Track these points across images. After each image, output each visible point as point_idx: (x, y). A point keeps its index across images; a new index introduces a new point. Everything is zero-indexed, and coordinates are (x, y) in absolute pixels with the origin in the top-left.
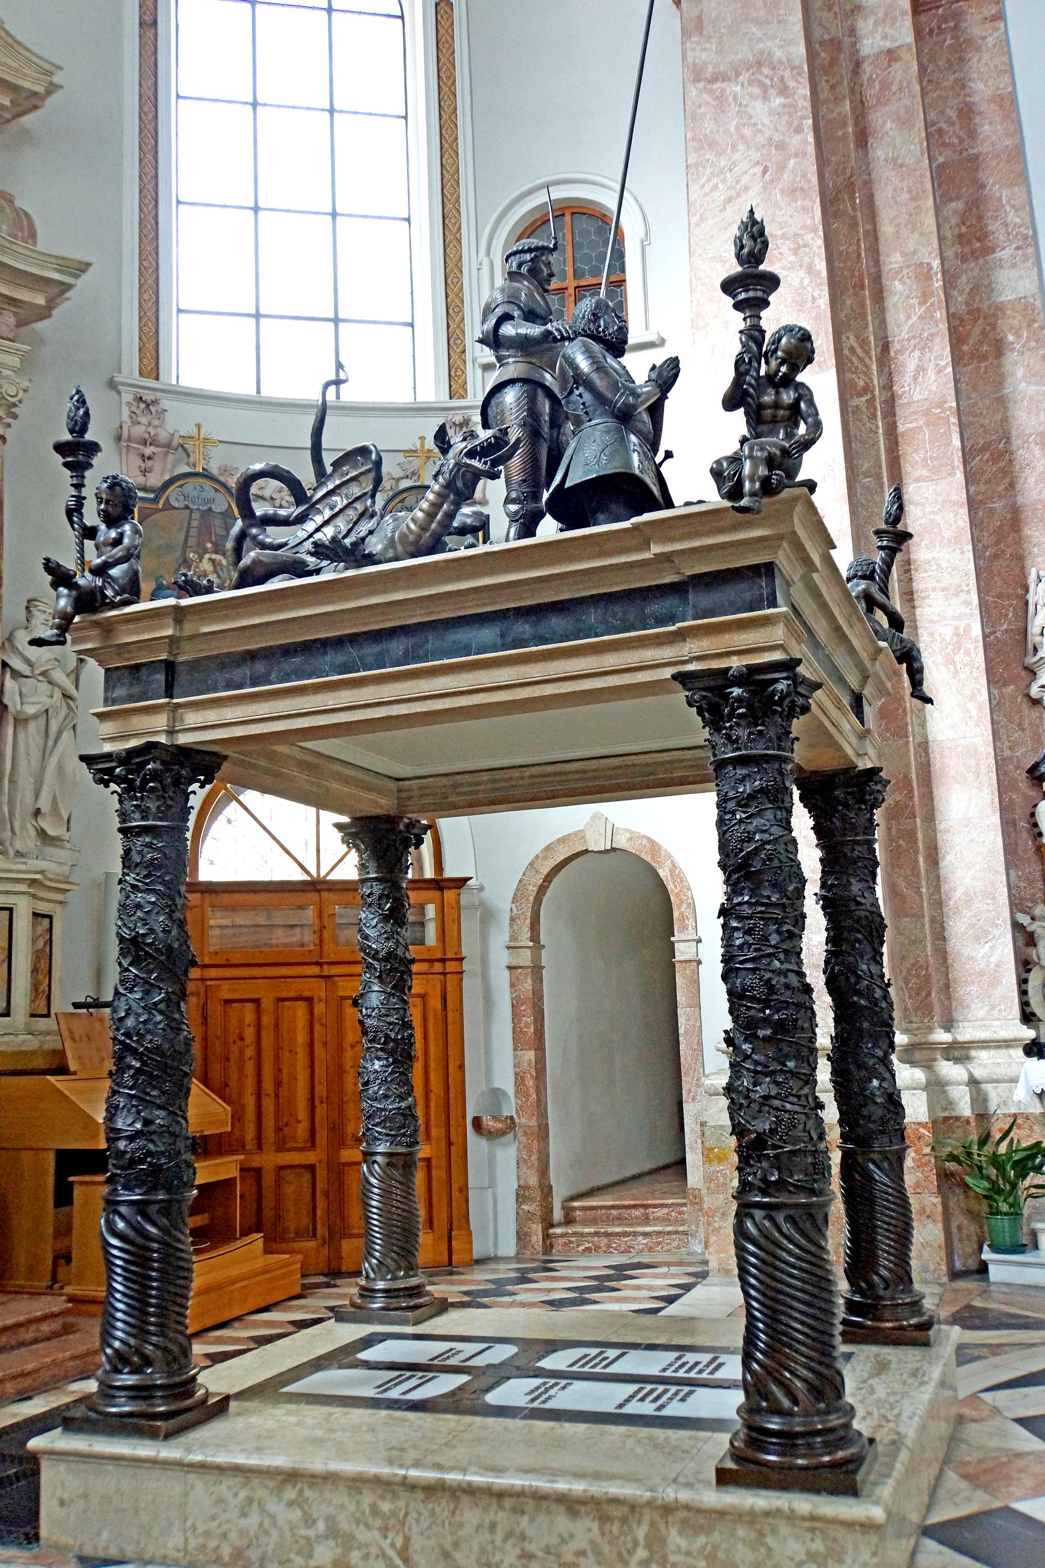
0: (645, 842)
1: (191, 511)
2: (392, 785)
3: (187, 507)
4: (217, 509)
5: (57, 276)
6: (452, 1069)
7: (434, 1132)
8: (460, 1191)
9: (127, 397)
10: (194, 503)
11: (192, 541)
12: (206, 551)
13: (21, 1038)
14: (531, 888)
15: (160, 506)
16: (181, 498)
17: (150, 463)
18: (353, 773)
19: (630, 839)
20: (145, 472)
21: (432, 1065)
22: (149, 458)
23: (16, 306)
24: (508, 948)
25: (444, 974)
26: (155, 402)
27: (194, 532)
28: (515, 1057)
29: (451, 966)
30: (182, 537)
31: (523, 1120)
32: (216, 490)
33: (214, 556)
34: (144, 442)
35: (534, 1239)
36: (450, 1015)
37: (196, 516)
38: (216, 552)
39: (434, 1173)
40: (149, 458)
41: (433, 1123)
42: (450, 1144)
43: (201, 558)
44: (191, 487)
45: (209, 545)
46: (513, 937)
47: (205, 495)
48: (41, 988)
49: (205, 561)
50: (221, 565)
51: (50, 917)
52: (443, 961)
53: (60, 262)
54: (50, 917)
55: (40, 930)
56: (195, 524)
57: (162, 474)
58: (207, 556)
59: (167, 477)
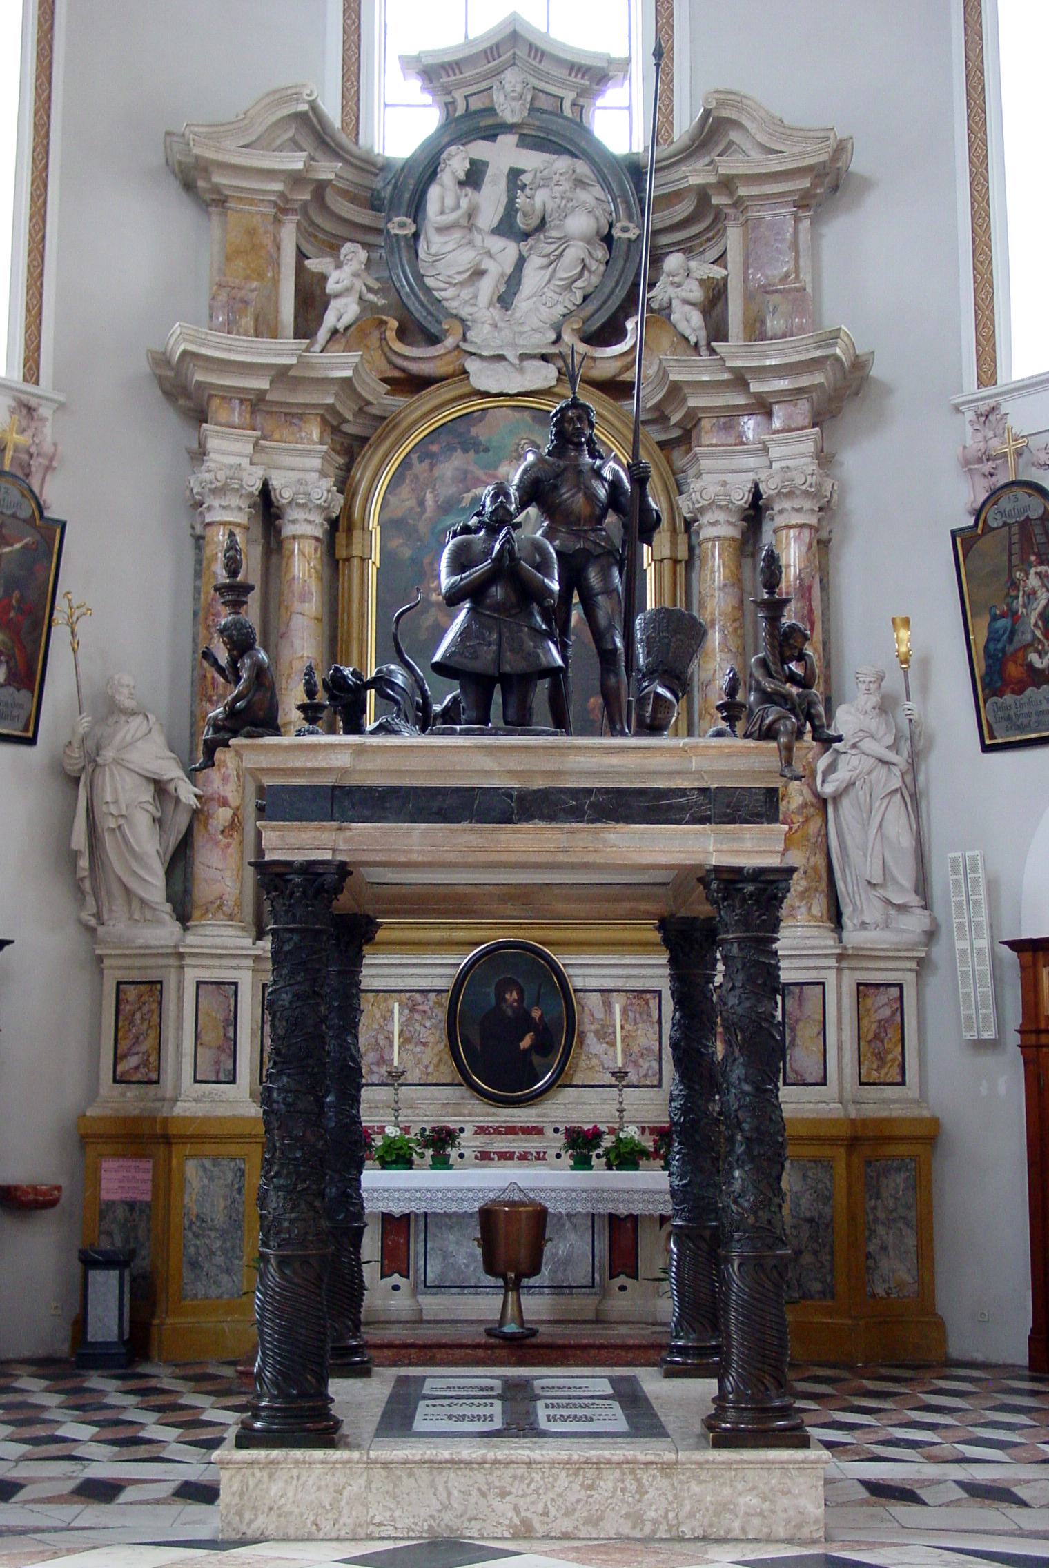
3: (1005, 524)
5: (818, 353)
9: (970, 415)
10: (1010, 516)
12: (1031, 565)
15: (979, 531)
16: (998, 517)
23: (806, 392)
26: (993, 409)
27: (1016, 548)
30: (1005, 558)
32: (1030, 495)
34: (980, 460)
37: (1015, 530)
38: (1041, 563)
43: (1027, 575)
44: (1005, 503)
45: (1033, 558)
47: (1020, 505)
49: (1032, 576)
56: (1015, 539)
58: (1033, 571)
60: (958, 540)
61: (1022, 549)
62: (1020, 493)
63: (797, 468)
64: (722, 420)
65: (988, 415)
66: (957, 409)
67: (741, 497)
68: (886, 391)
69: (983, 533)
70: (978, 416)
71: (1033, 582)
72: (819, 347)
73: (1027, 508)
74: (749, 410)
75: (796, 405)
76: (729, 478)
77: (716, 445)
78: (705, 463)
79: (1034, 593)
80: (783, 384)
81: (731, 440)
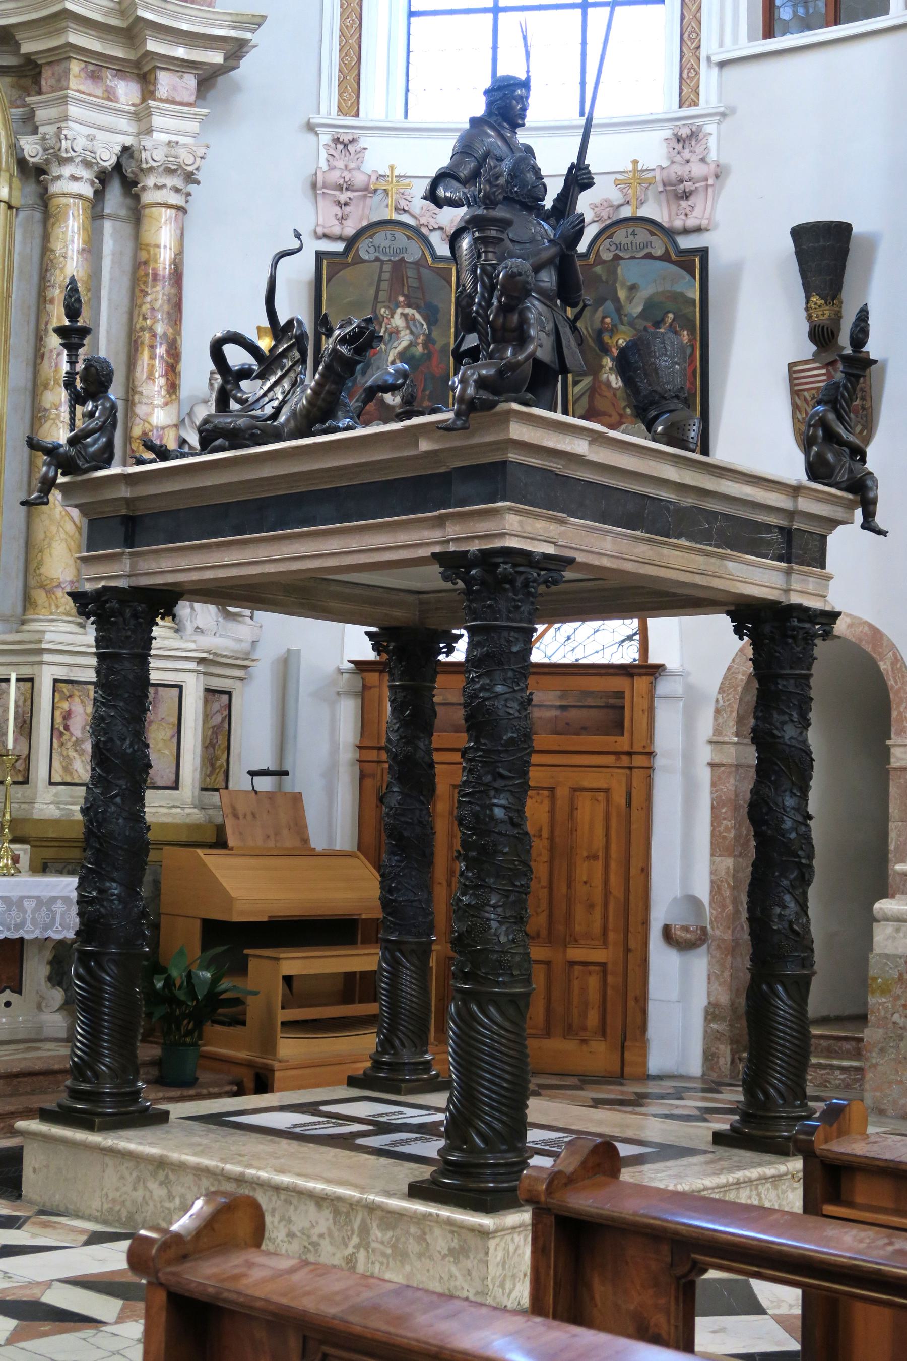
0: (866, 629)
1: (382, 262)
2: (411, 598)
3: (377, 259)
4: (409, 258)
5: (233, 33)
6: (633, 871)
7: (611, 936)
8: (636, 999)
9: (325, 138)
10: (385, 254)
11: (382, 296)
12: (398, 306)
13: (187, 811)
14: (740, 677)
15: (349, 260)
16: (372, 250)
17: (347, 209)
18: (357, 591)
19: (850, 626)
20: (342, 219)
21: (613, 865)
22: (346, 204)
23: (196, 68)
24: (711, 742)
25: (630, 768)
26: (353, 141)
27: (385, 285)
28: (712, 863)
29: (638, 761)
30: (372, 292)
31: (718, 933)
32: (409, 238)
33: (407, 310)
34: (340, 188)
35: (722, 1061)
36: (635, 814)
37: (387, 267)
38: (409, 306)
39: (610, 979)
40: (346, 204)
41: (611, 926)
42: (627, 950)
44: (381, 238)
45: (401, 299)
46: (717, 731)
48: (218, 763)
49: (397, 316)
50: (414, 319)
51: (229, 693)
52: (630, 754)
53: (234, 18)
54: (229, 693)
55: (216, 706)
57: (361, 219)
58: (399, 311)
59: (365, 223)
60: (325, 262)
61: (391, 286)
62: (400, 235)
63: (185, 145)
64: (91, 67)
65: (343, 144)
66: (311, 128)
67: (108, 159)
68: (236, 88)
69: (354, 263)
70: (337, 141)
71: (398, 321)
72: (233, 28)
73: (404, 250)
74: (123, 69)
75: (181, 77)
76: (100, 135)
77: (83, 93)
78: (73, 110)
79: (397, 332)
80: (181, 52)
81: (99, 92)
